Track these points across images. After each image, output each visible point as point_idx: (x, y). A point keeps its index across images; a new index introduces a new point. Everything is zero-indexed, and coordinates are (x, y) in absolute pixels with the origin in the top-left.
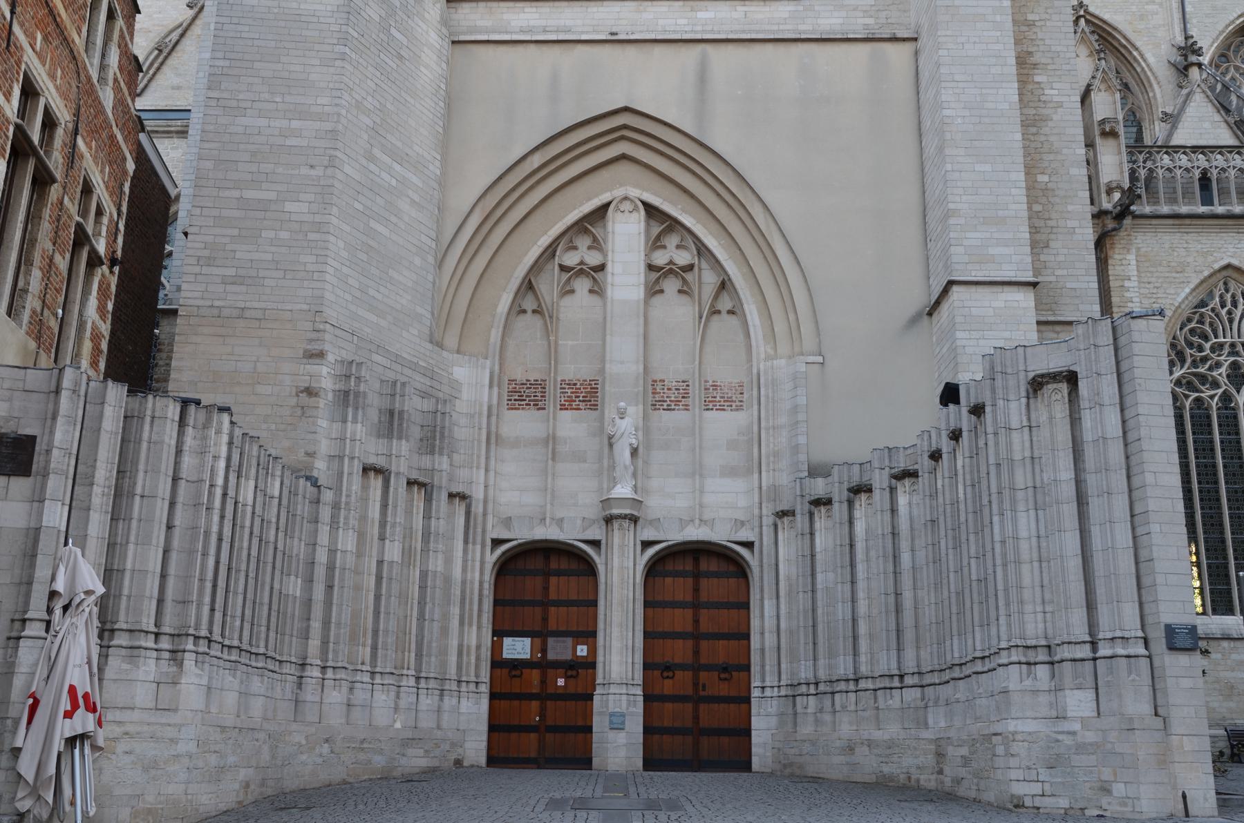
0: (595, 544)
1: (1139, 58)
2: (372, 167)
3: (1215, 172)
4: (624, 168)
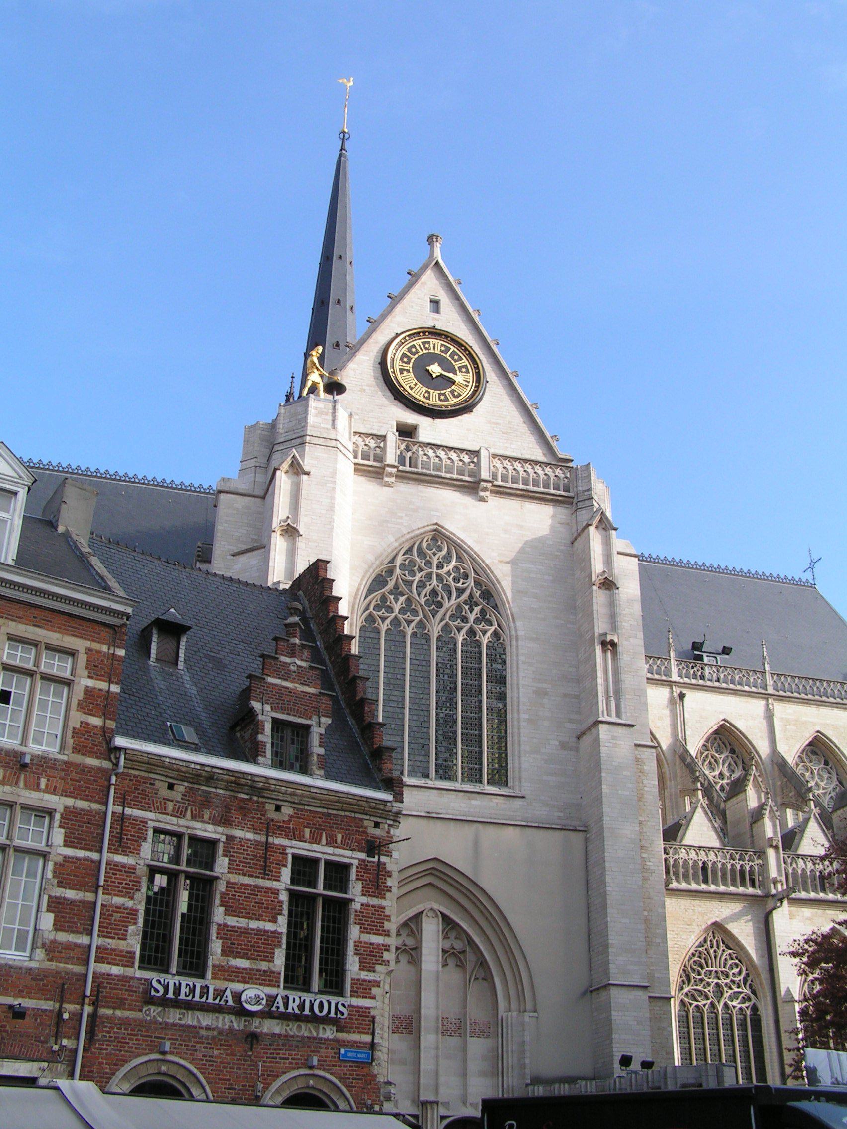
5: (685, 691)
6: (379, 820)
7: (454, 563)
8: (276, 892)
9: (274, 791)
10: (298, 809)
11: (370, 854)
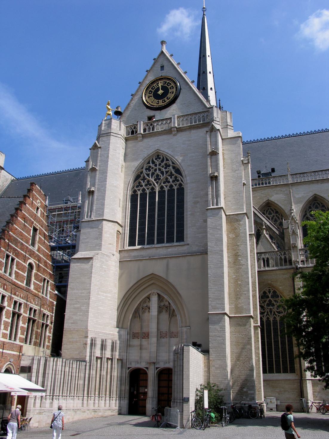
0: (147, 368)
2: (99, 296)
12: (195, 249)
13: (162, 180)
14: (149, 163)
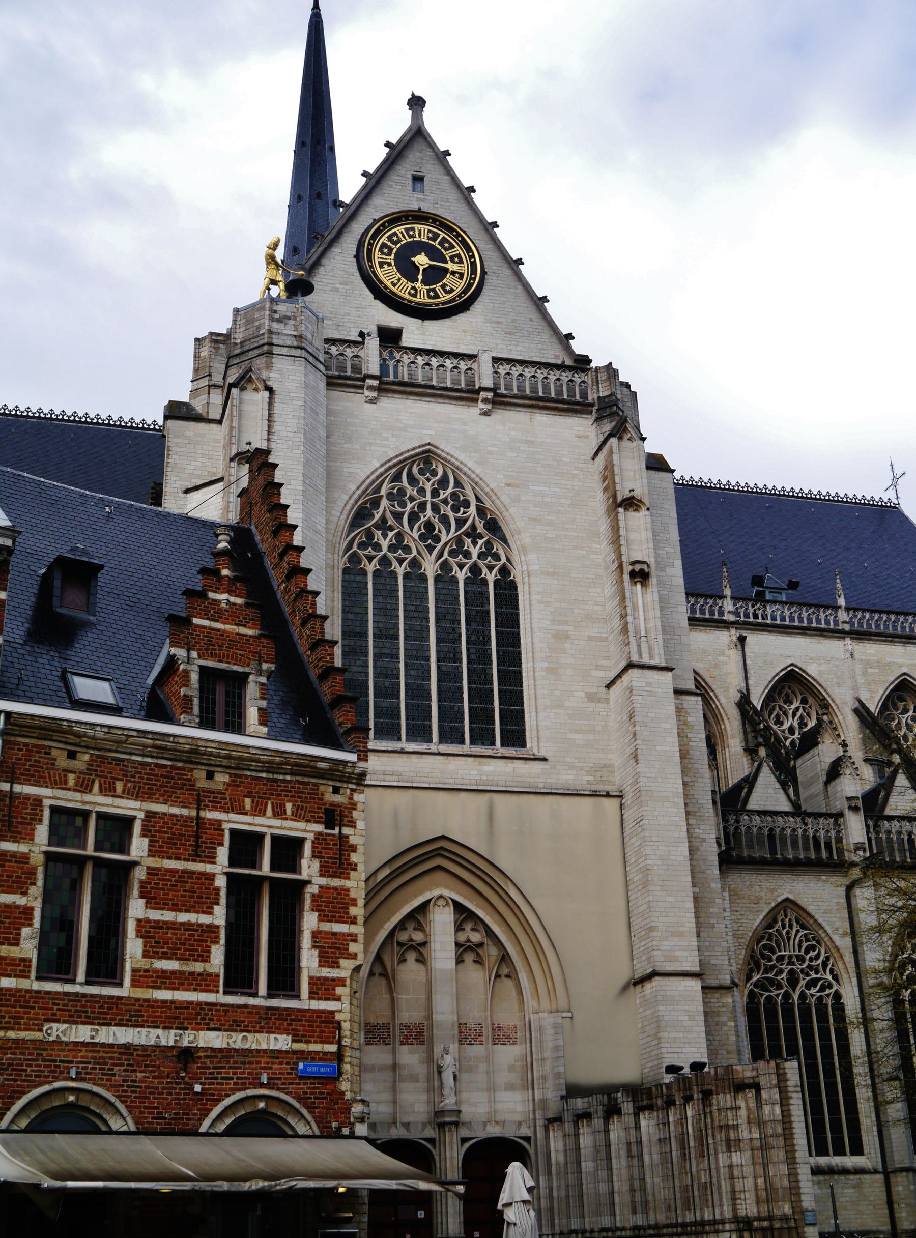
0: (432, 1141)
1: (714, 697)
3: (778, 830)
4: (439, 876)
5: (744, 633)
6: (338, 784)
7: (450, 490)
8: (211, 877)
9: (204, 754)
10: (236, 775)
11: (330, 825)
12: (566, 778)
13: (446, 544)
14: (397, 478)
